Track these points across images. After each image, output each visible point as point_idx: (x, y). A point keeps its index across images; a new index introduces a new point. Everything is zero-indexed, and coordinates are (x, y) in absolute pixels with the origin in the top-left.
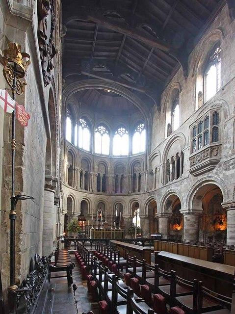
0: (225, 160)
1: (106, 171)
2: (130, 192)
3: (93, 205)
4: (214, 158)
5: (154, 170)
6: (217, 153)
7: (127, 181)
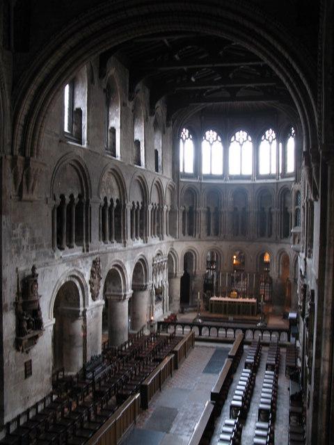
2: (279, 237)
7: (276, 219)
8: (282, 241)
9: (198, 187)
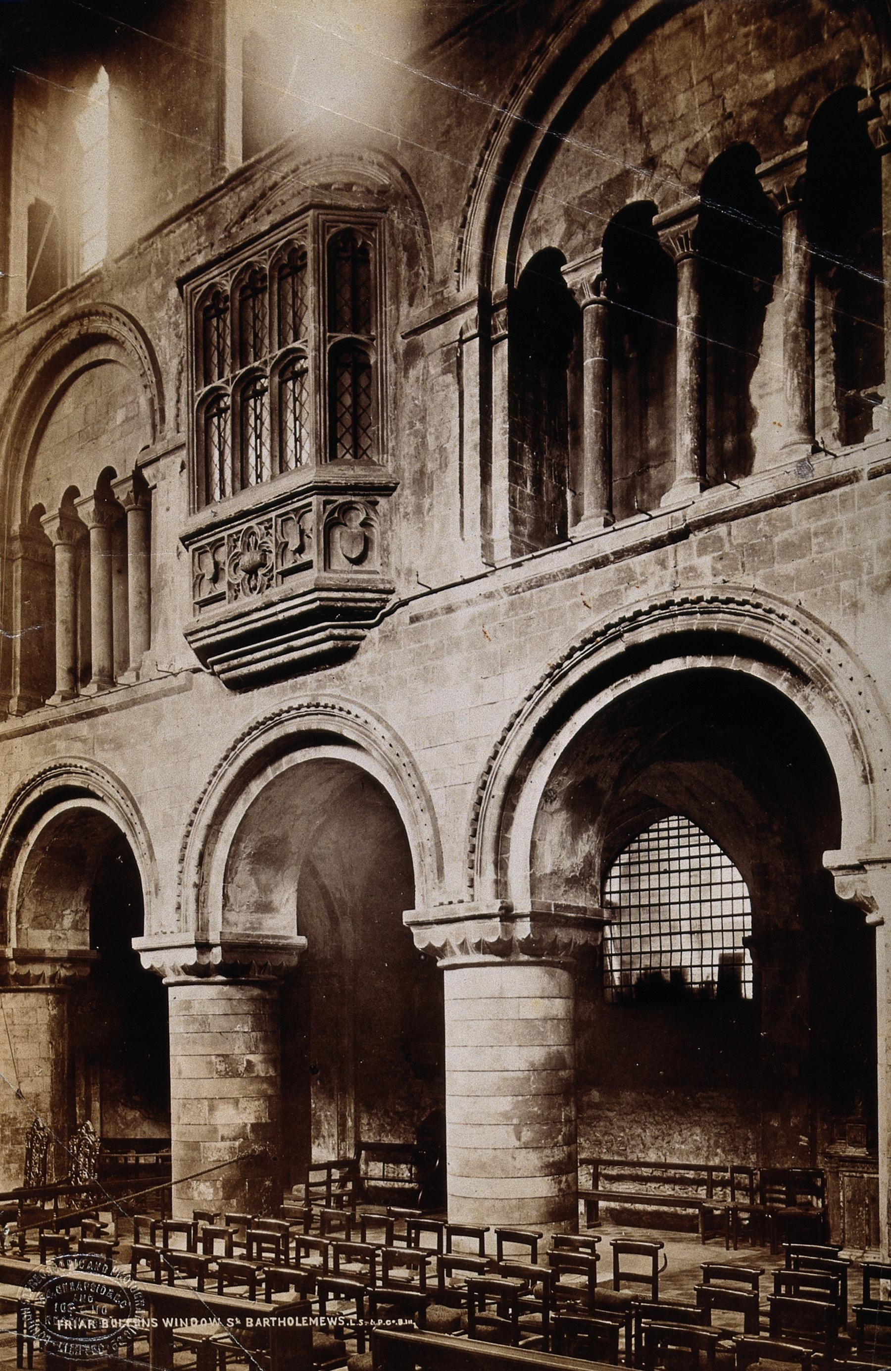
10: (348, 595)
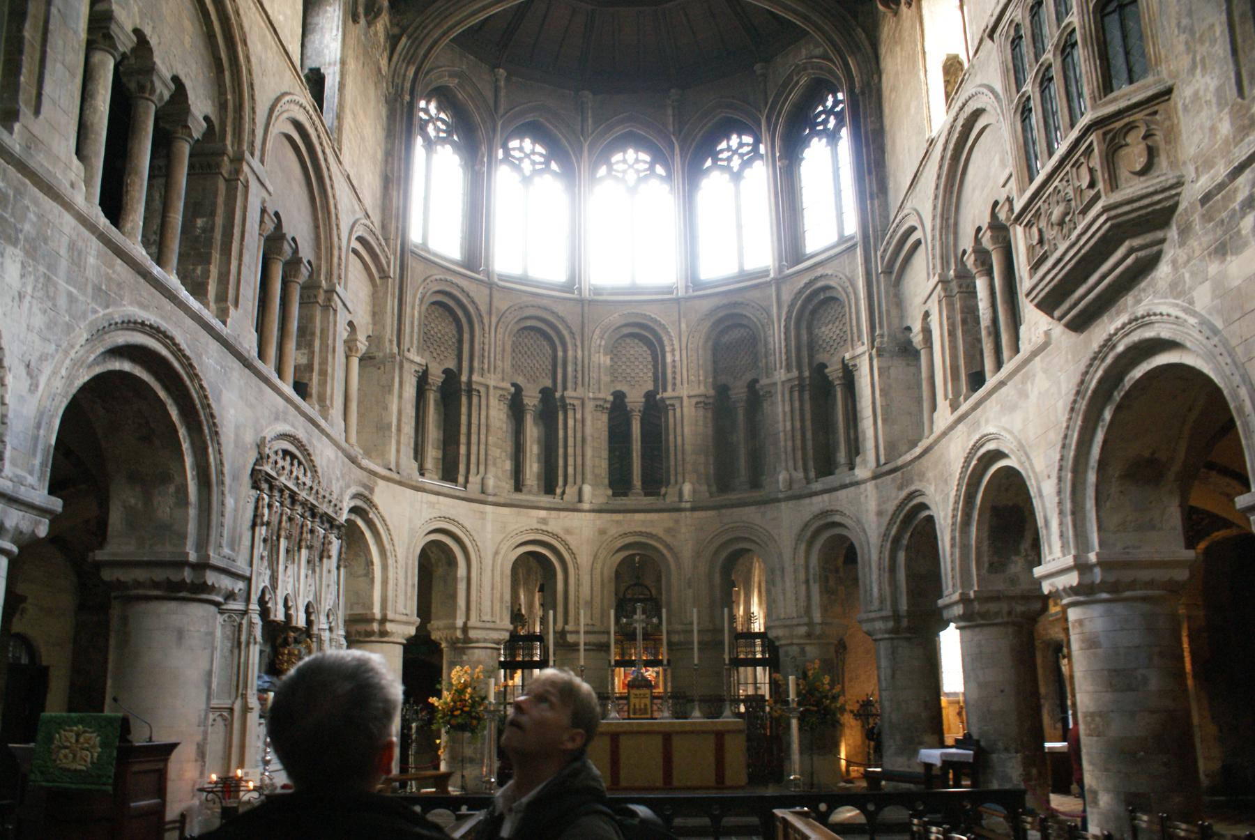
0: (1204, 183)
1: (660, 379)
3: (586, 579)
4: (1132, 188)
5: (917, 327)
6: (1152, 153)
8: (817, 486)
9: (480, 296)
10: (1136, 205)
